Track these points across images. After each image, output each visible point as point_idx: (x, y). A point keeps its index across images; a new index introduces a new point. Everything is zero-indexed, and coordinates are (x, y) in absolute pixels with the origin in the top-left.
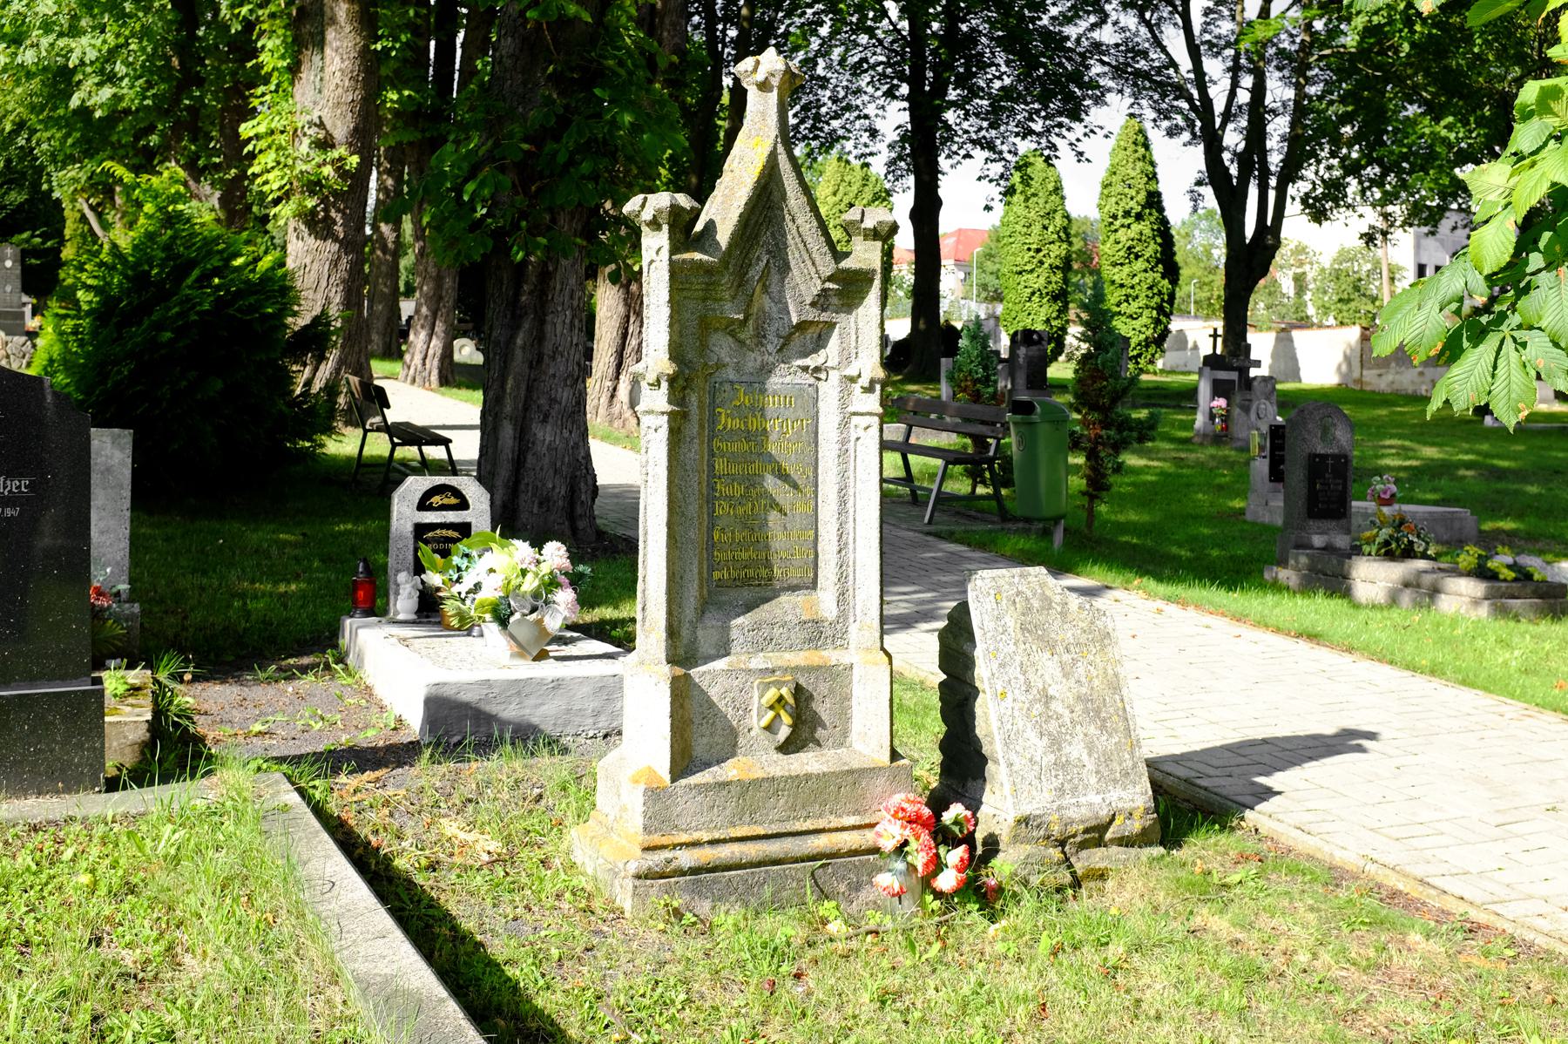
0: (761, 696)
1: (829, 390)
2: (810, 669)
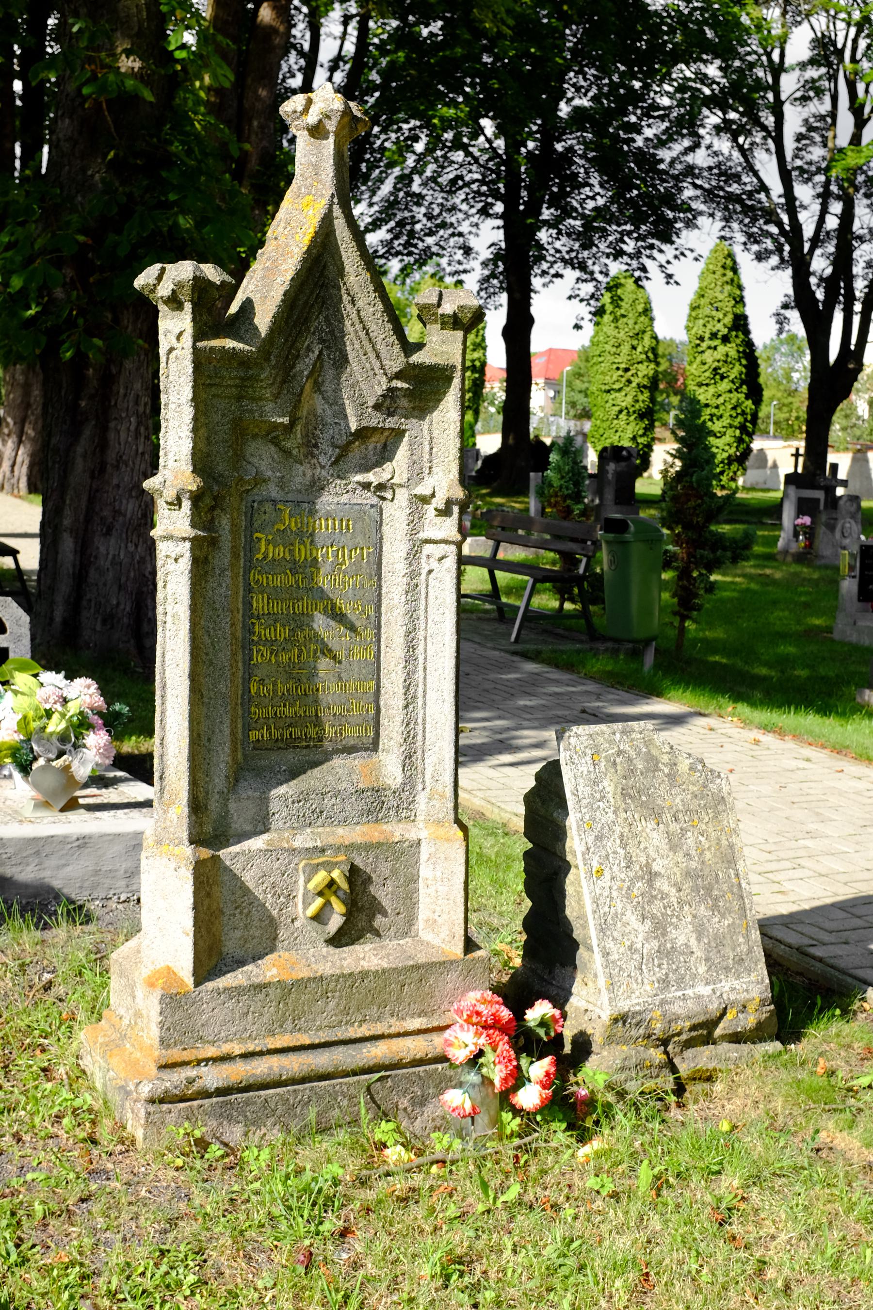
1: (396, 513)
2: (367, 847)
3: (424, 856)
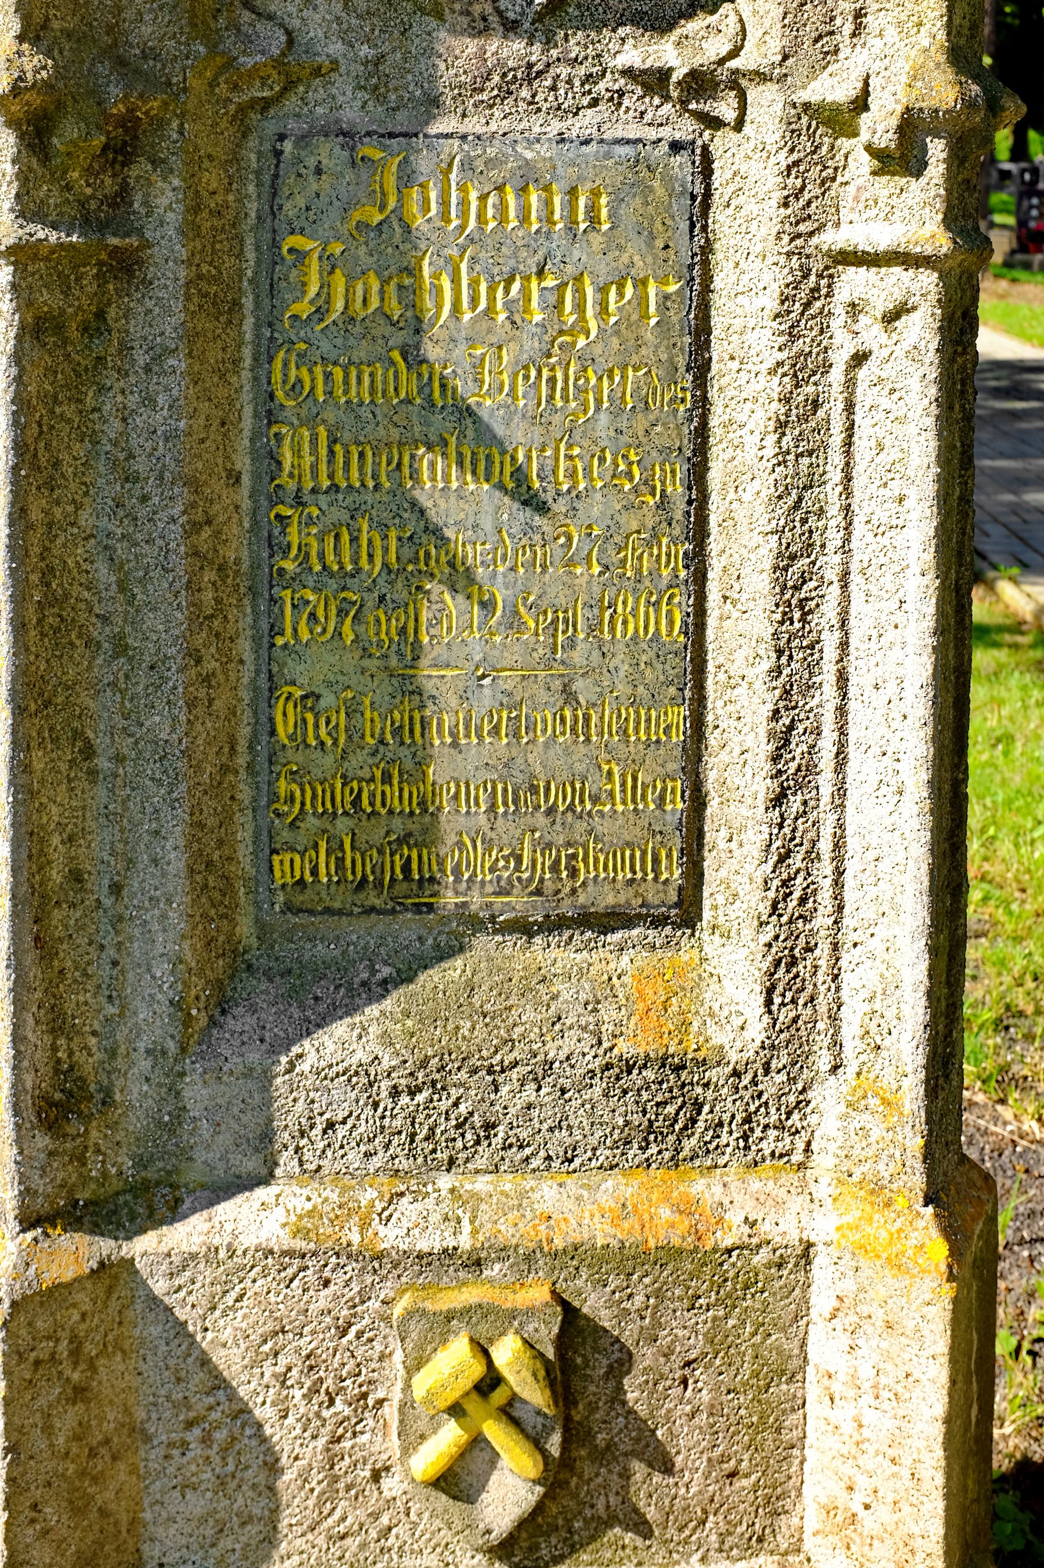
0: (415, 1365)
1: (751, 164)
2: (625, 1261)
3: (821, 1300)
